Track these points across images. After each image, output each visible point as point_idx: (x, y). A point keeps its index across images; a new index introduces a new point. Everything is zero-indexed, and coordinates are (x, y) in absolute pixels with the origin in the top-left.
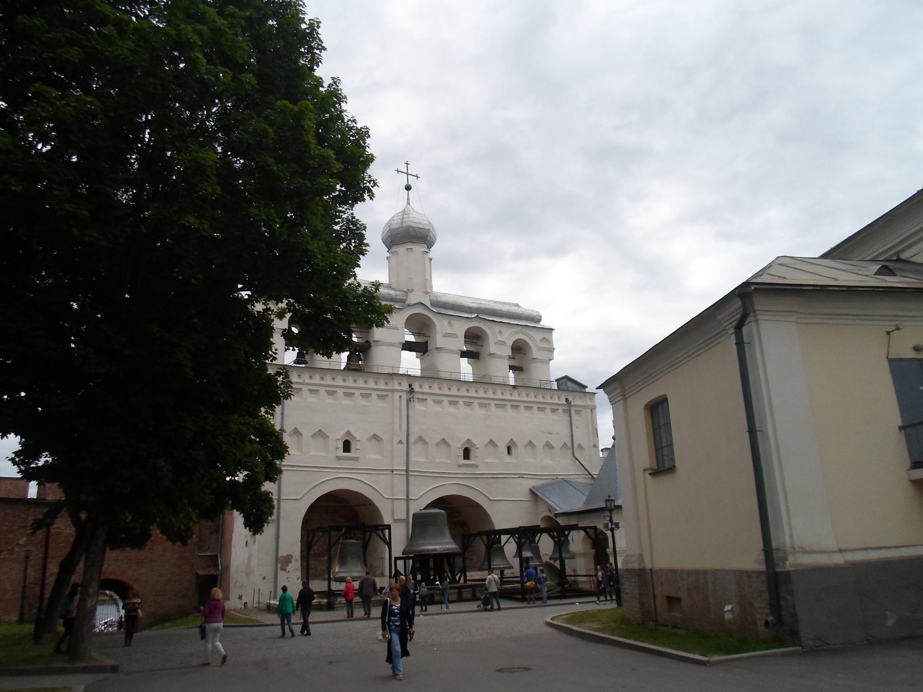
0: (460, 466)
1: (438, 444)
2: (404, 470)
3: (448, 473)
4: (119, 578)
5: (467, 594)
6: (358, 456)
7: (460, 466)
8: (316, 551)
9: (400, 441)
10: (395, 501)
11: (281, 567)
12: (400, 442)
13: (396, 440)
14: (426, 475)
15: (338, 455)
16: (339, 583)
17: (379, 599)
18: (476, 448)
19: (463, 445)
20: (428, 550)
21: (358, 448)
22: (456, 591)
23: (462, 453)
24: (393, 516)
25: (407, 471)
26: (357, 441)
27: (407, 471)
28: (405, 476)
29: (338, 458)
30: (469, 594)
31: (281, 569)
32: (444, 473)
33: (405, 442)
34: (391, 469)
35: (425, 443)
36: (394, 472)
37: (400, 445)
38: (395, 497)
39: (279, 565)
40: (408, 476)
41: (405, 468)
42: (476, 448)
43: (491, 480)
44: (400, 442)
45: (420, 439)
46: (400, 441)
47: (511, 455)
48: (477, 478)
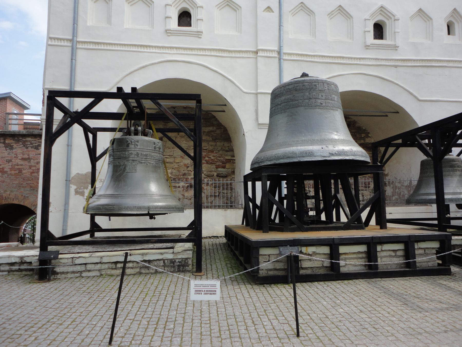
0: (367, 47)
1: (331, 15)
2: (274, 51)
3: (349, 58)
4: (22, 204)
5: (390, 256)
6: (199, 29)
7: (367, 47)
8: (170, 175)
9: (269, 7)
10: (259, 95)
11: (75, 190)
12: (269, 9)
13: (262, 6)
14: (313, 60)
15: (168, 28)
16: (108, 217)
17: (170, 256)
18: (395, 20)
19: (372, 15)
20: (294, 155)
21: (199, 17)
22: (363, 248)
23: (371, 28)
24: (257, 119)
25: (279, 53)
26: (198, 7)
27: (279, 53)
28: (277, 59)
29: (168, 32)
30: (396, 256)
31: (77, 192)
32: (340, 57)
33: (276, 10)
34: (255, 50)
35: (310, 12)
36: (258, 54)
37: (267, 14)
38: (259, 91)
39: (73, 188)
40: (280, 59)
41: (276, 48)
42: (395, 20)
43: (421, 71)
44: (269, 9)
45: (303, 7)
46: (269, 7)
47: (454, 34)
48: (396, 66)
